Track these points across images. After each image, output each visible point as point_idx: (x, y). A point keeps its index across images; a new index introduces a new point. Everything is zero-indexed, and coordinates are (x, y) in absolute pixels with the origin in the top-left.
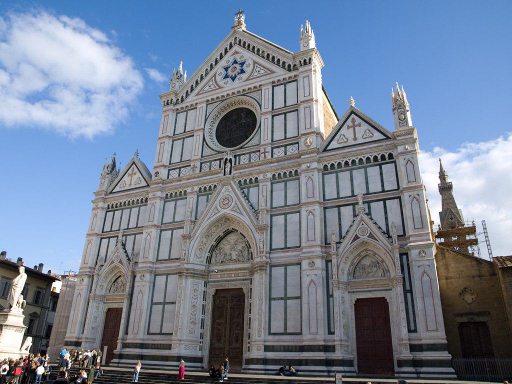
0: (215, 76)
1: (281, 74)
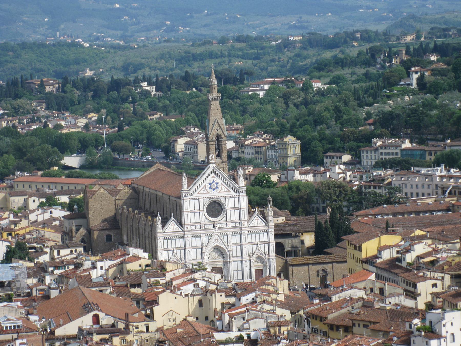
0: (205, 186)
1: (233, 193)
